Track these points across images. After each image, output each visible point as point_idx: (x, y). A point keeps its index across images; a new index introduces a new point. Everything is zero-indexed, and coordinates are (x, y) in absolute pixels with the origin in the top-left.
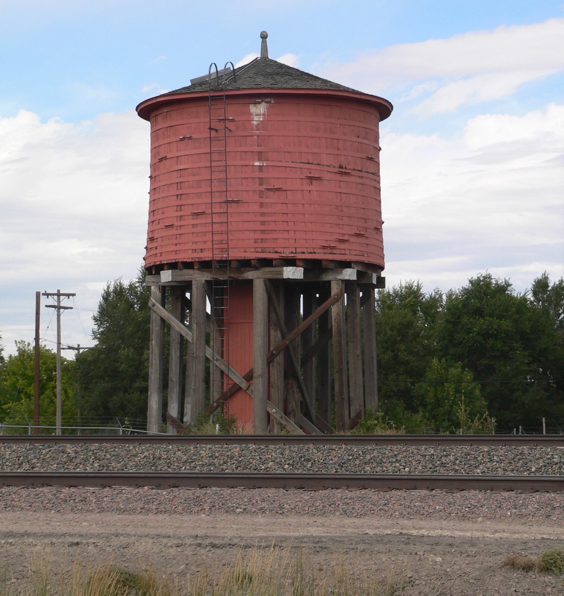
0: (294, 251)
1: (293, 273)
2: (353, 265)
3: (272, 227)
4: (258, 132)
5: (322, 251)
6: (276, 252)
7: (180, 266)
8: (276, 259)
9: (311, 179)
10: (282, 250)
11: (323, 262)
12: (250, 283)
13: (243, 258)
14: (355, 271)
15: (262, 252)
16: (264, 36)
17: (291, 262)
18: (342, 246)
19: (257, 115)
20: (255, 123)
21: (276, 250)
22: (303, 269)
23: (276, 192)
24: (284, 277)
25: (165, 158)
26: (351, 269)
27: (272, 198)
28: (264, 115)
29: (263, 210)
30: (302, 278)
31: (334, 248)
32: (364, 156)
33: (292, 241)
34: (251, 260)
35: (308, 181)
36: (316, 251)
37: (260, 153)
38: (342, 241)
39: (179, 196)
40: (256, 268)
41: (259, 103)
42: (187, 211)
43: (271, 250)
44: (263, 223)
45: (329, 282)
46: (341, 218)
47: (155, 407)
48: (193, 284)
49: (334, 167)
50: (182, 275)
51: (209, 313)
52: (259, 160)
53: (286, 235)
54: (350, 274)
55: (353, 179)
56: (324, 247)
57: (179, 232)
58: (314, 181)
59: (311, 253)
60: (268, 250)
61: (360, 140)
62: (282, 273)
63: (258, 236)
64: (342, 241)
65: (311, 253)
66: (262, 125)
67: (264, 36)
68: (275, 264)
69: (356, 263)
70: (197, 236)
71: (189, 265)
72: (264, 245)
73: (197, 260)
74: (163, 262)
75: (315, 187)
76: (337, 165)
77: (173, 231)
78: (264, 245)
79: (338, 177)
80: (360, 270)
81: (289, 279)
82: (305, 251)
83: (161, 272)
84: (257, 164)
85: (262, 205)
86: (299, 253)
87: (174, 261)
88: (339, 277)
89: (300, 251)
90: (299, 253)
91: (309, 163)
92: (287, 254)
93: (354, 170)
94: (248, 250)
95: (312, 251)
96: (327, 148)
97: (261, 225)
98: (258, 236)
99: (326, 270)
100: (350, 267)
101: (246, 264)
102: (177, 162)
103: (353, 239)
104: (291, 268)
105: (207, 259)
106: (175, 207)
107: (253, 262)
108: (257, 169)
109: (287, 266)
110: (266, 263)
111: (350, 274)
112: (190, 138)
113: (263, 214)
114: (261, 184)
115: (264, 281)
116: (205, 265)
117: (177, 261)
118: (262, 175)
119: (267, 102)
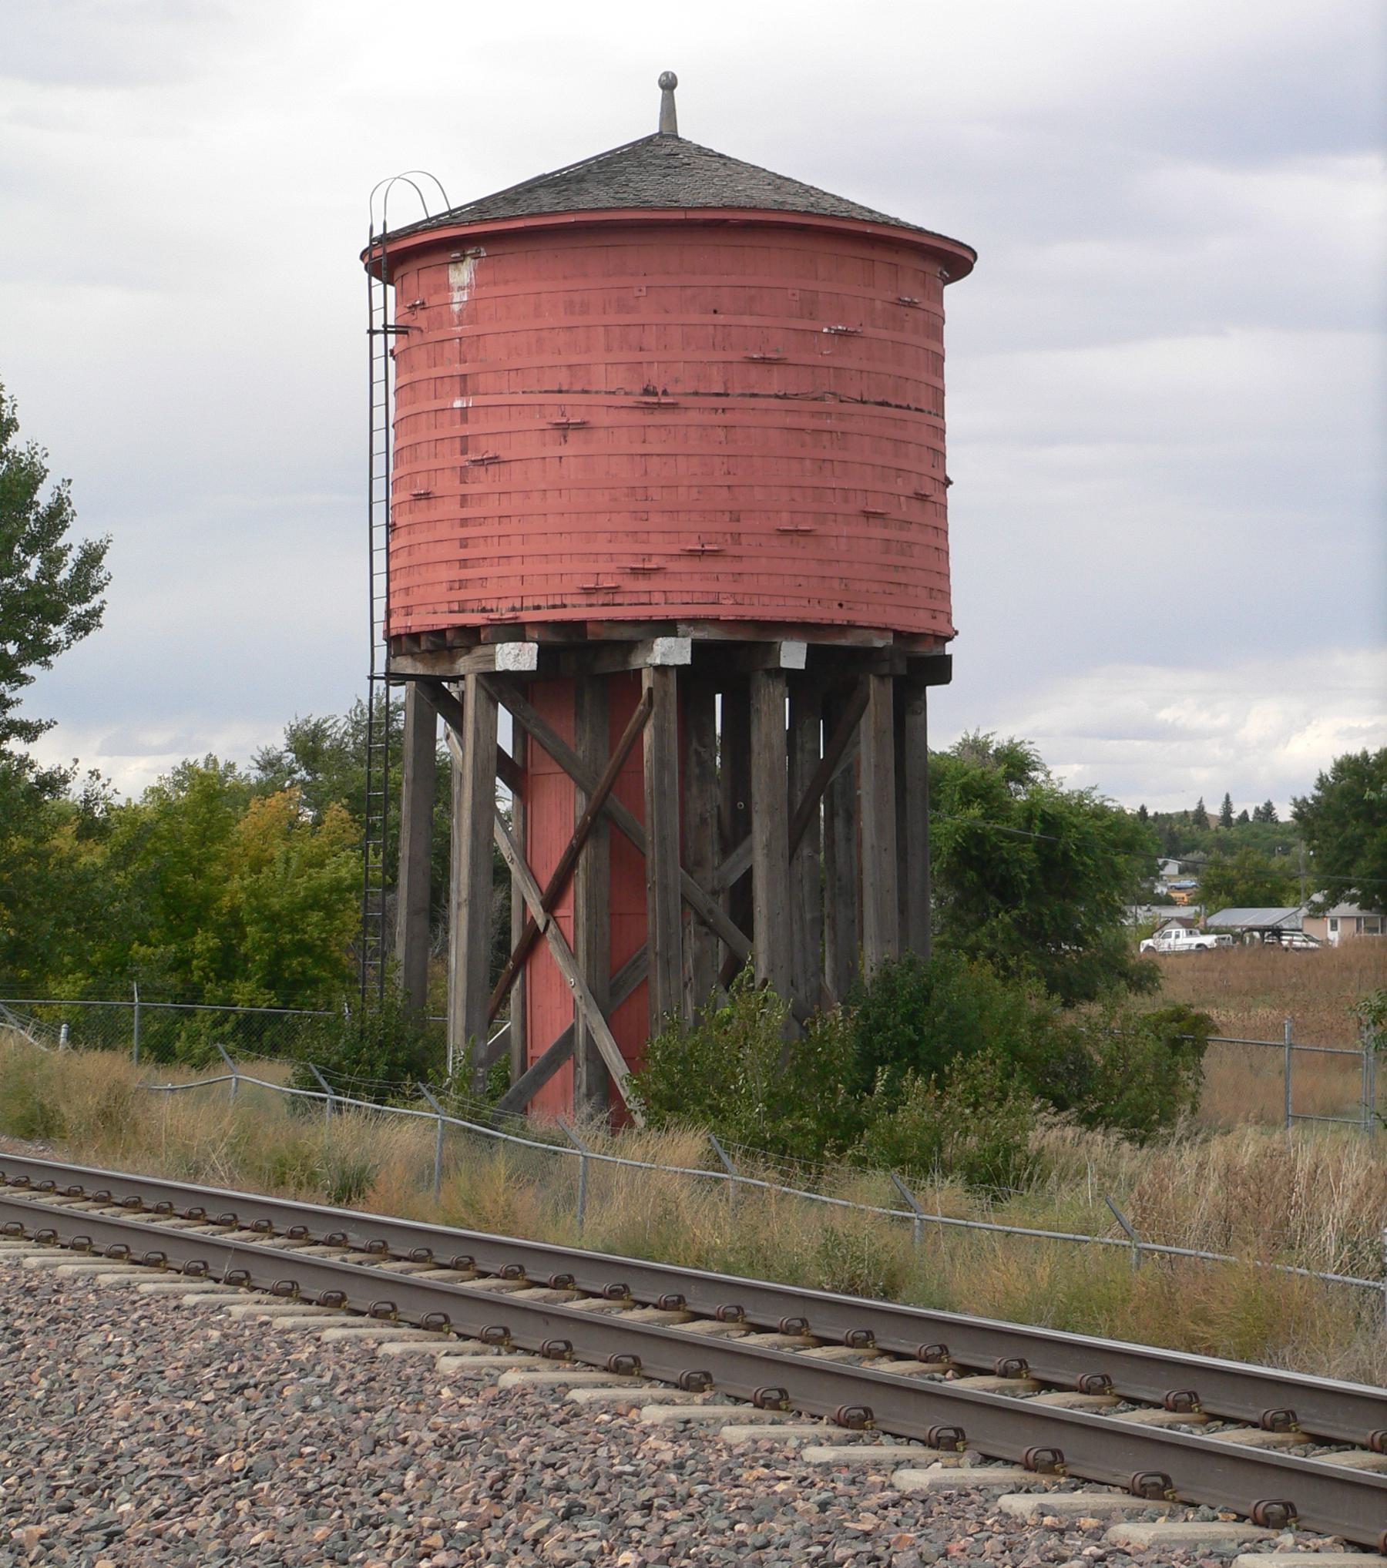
2: (681, 628)
4: (459, 329)
5: (582, 600)
6: (484, 610)
8: (485, 626)
9: (564, 428)
11: (589, 627)
14: (688, 641)
15: (459, 612)
16: (669, 84)
17: (515, 631)
18: (642, 585)
19: (461, 288)
20: (456, 308)
22: (536, 646)
23: (490, 467)
26: (673, 639)
27: (483, 482)
28: (469, 286)
29: (467, 513)
30: (534, 668)
31: (615, 590)
32: (735, 356)
33: (516, 582)
34: (444, 630)
35: (558, 434)
36: (568, 601)
44: (464, 543)
45: (638, 672)
46: (645, 516)
49: (626, 394)
51: (509, 751)
52: (463, 394)
53: (503, 569)
55: (693, 417)
56: (588, 591)
58: (571, 435)
59: (554, 607)
60: (470, 606)
61: (721, 319)
62: (492, 659)
63: (456, 573)
64: (646, 572)
65: (554, 607)
66: (471, 313)
67: (669, 84)
69: (693, 622)
72: (462, 595)
75: (574, 446)
76: (638, 388)
78: (462, 595)
79: (638, 417)
82: (542, 602)
84: (458, 404)
85: (464, 500)
86: (528, 609)
88: (649, 661)
90: (528, 609)
91: (560, 392)
93: (696, 394)
95: (558, 603)
96: (609, 349)
98: (456, 573)
99: (629, 647)
104: (512, 645)
107: (449, 635)
109: (502, 643)
110: (471, 637)
113: (464, 522)
114: (464, 452)
119: (476, 257)
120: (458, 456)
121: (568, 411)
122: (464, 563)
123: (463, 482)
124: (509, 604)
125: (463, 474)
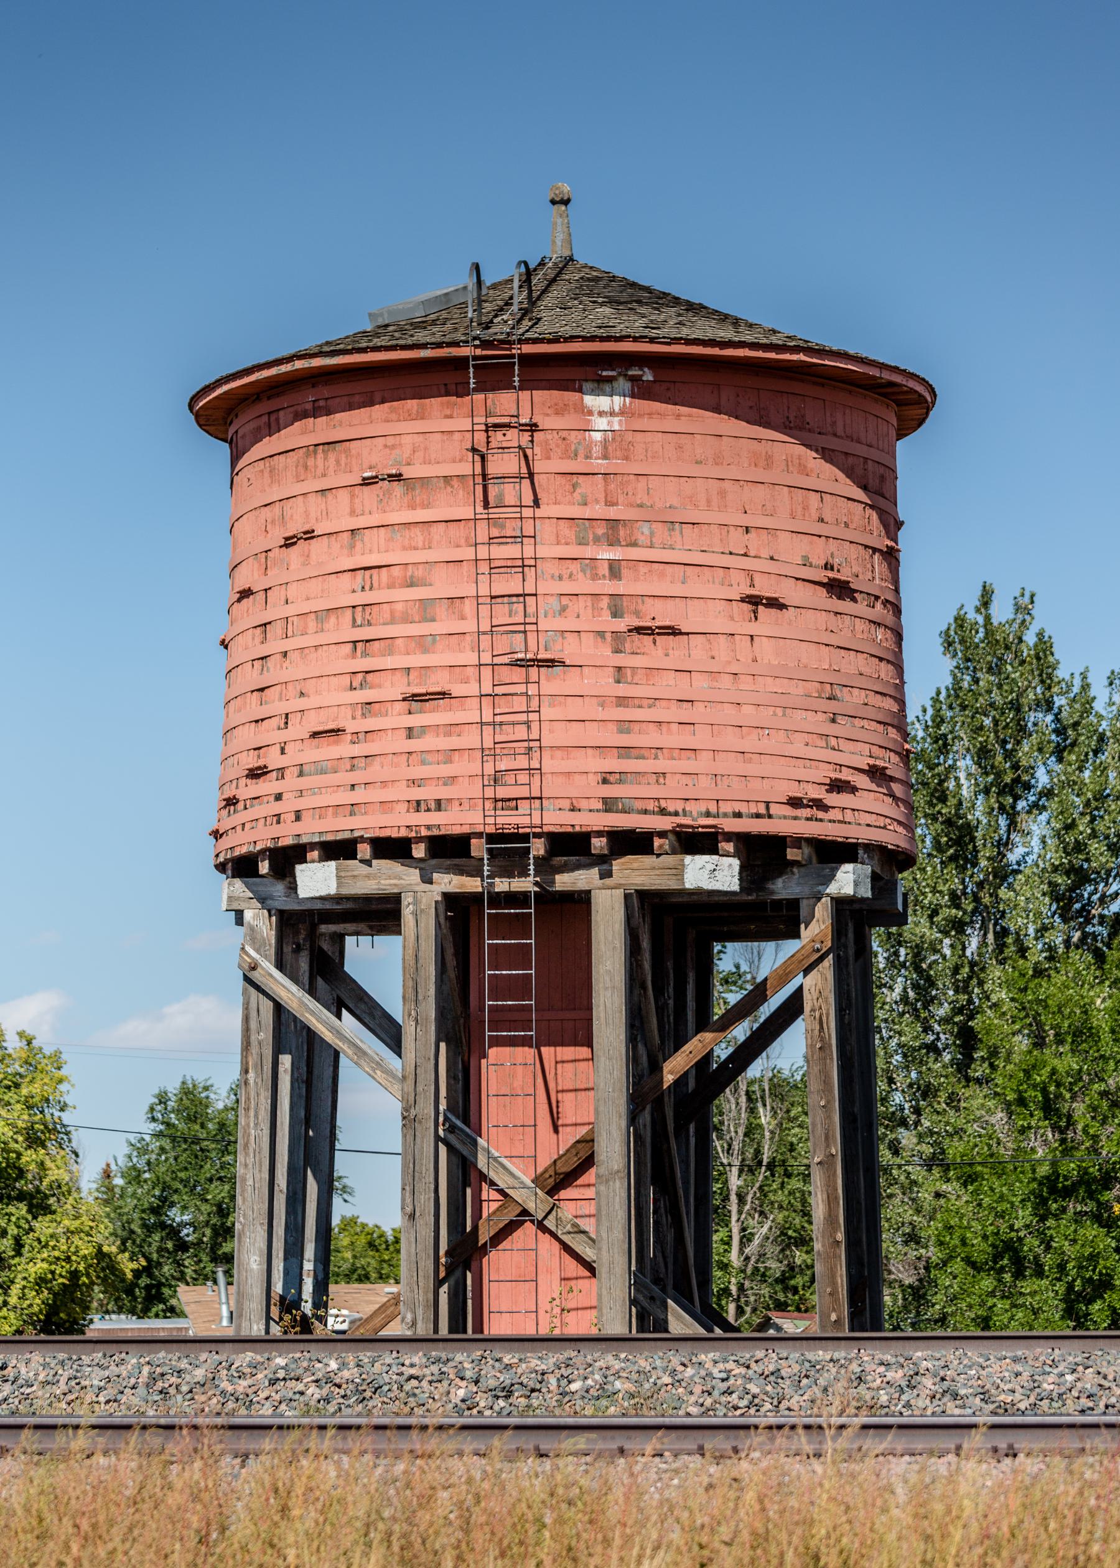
0: (713, 809)
1: (715, 874)
3: (649, 738)
5: (788, 811)
6: (663, 812)
7: (364, 850)
8: (662, 834)
9: (754, 601)
10: (679, 806)
12: (581, 901)
13: (570, 829)
19: (601, 414)
21: (663, 804)
23: (658, 638)
24: (688, 886)
25: (309, 535)
29: (622, 690)
33: (705, 782)
35: (747, 607)
37: (613, 523)
38: (837, 786)
39: (359, 645)
40: (603, 861)
41: (610, 380)
42: (393, 689)
43: (651, 806)
44: (625, 726)
47: (255, 1266)
48: (404, 903)
50: (368, 877)
54: (847, 880)
56: (795, 802)
57: (357, 750)
60: (639, 805)
63: (612, 764)
68: (661, 846)
69: (869, 847)
70: (423, 763)
71: (392, 848)
73: (424, 832)
74: (305, 840)
77: (344, 749)
80: (878, 871)
81: (699, 892)
82: (743, 808)
83: (299, 868)
86: (725, 815)
87: (347, 835)
89: (729, 810)
90: (725, 815)
92: (696, 819)
94: (584, 804)
97: (620, 731)
100: (853, 859)
101: (570, 846)
102: (353, 547)
103: (862, 781)
104: (706, 858)
105: (457, 830)
106: (347, 678)
108: (604, 569)
111: (847, 880)
112: (397, 477)
113: (622, 701)
115: (627, 897)
116: (449, 849)
117: (356, 834)
118: (620, 587)
120: (606, 616)
121: (757, 578)
122: (625, 751)
123: (617, 651)
124: (702, 807)
125: (618, 642)
